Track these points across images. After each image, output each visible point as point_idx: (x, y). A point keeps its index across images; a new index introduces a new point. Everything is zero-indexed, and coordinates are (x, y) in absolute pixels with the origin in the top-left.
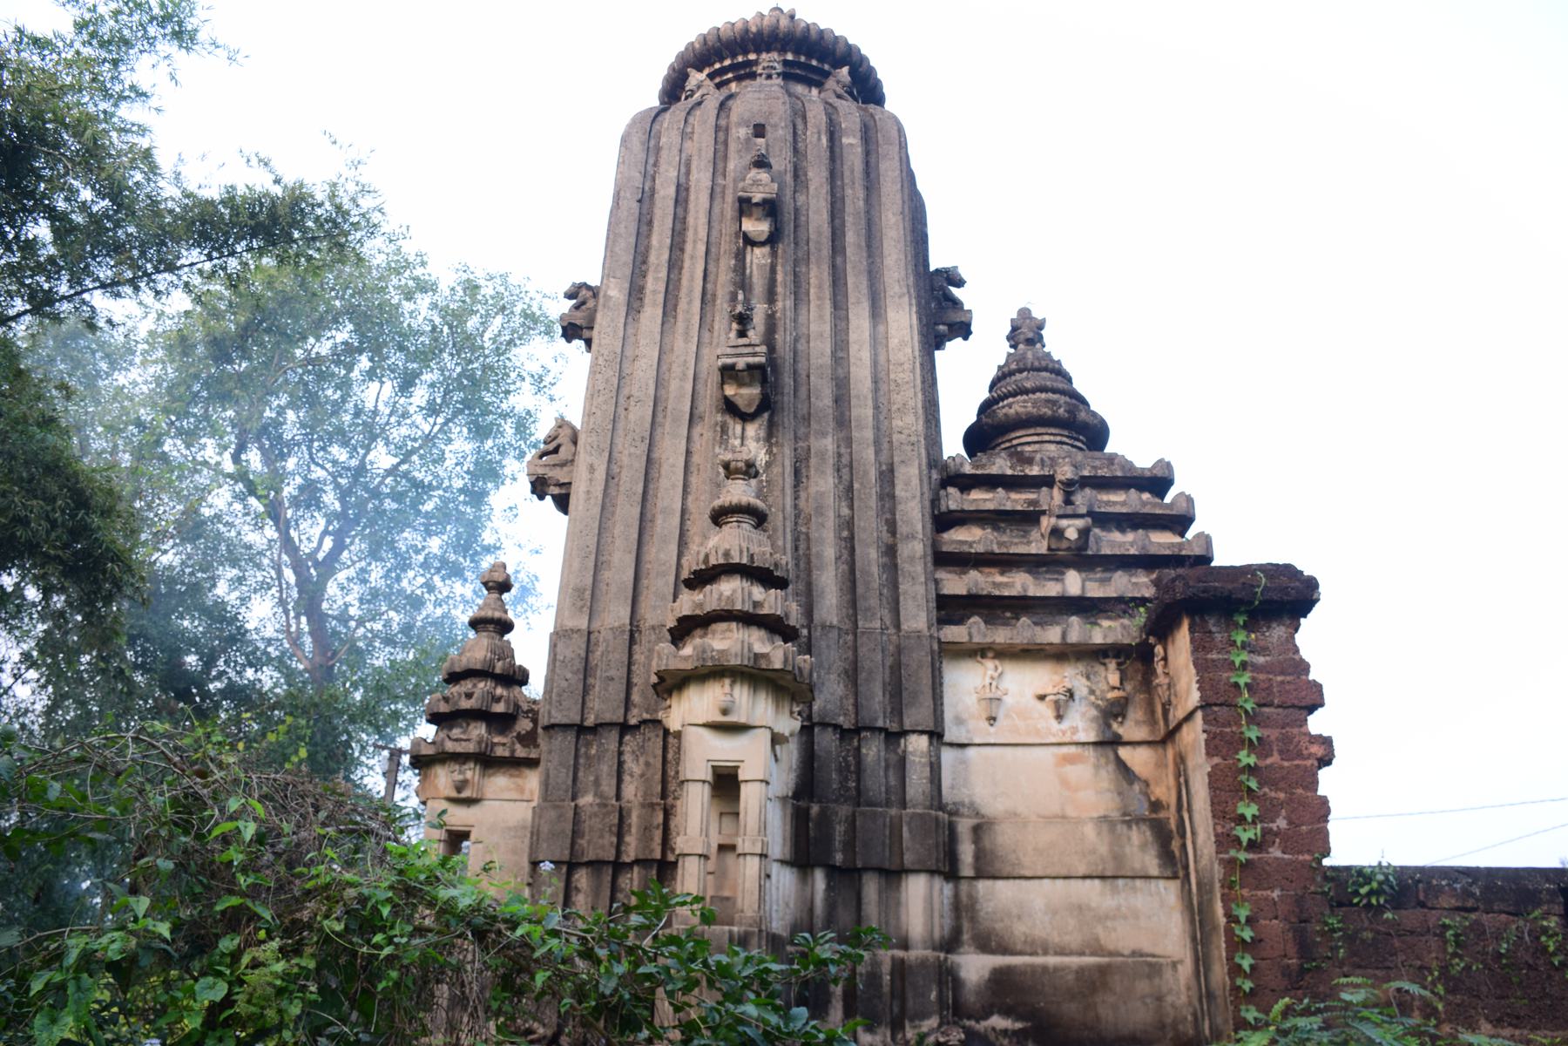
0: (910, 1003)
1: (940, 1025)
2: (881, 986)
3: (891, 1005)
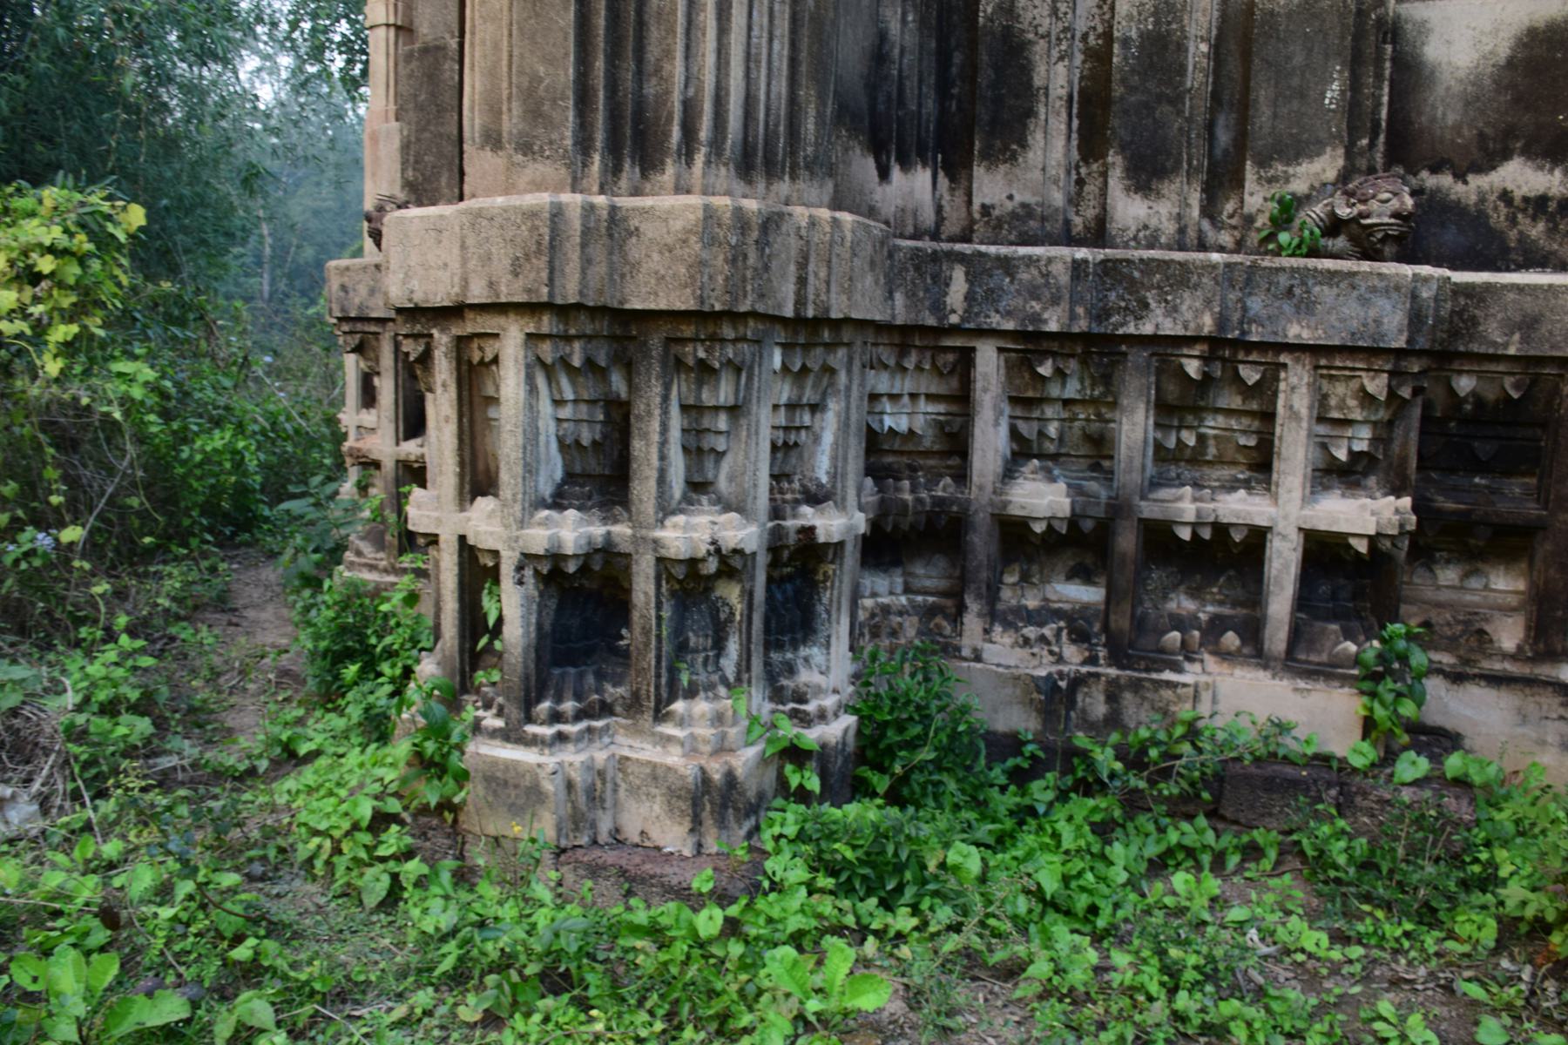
0: (1263, 117)
1: (1344, 177)
2: (1182, 70)
3: (1210, 127)
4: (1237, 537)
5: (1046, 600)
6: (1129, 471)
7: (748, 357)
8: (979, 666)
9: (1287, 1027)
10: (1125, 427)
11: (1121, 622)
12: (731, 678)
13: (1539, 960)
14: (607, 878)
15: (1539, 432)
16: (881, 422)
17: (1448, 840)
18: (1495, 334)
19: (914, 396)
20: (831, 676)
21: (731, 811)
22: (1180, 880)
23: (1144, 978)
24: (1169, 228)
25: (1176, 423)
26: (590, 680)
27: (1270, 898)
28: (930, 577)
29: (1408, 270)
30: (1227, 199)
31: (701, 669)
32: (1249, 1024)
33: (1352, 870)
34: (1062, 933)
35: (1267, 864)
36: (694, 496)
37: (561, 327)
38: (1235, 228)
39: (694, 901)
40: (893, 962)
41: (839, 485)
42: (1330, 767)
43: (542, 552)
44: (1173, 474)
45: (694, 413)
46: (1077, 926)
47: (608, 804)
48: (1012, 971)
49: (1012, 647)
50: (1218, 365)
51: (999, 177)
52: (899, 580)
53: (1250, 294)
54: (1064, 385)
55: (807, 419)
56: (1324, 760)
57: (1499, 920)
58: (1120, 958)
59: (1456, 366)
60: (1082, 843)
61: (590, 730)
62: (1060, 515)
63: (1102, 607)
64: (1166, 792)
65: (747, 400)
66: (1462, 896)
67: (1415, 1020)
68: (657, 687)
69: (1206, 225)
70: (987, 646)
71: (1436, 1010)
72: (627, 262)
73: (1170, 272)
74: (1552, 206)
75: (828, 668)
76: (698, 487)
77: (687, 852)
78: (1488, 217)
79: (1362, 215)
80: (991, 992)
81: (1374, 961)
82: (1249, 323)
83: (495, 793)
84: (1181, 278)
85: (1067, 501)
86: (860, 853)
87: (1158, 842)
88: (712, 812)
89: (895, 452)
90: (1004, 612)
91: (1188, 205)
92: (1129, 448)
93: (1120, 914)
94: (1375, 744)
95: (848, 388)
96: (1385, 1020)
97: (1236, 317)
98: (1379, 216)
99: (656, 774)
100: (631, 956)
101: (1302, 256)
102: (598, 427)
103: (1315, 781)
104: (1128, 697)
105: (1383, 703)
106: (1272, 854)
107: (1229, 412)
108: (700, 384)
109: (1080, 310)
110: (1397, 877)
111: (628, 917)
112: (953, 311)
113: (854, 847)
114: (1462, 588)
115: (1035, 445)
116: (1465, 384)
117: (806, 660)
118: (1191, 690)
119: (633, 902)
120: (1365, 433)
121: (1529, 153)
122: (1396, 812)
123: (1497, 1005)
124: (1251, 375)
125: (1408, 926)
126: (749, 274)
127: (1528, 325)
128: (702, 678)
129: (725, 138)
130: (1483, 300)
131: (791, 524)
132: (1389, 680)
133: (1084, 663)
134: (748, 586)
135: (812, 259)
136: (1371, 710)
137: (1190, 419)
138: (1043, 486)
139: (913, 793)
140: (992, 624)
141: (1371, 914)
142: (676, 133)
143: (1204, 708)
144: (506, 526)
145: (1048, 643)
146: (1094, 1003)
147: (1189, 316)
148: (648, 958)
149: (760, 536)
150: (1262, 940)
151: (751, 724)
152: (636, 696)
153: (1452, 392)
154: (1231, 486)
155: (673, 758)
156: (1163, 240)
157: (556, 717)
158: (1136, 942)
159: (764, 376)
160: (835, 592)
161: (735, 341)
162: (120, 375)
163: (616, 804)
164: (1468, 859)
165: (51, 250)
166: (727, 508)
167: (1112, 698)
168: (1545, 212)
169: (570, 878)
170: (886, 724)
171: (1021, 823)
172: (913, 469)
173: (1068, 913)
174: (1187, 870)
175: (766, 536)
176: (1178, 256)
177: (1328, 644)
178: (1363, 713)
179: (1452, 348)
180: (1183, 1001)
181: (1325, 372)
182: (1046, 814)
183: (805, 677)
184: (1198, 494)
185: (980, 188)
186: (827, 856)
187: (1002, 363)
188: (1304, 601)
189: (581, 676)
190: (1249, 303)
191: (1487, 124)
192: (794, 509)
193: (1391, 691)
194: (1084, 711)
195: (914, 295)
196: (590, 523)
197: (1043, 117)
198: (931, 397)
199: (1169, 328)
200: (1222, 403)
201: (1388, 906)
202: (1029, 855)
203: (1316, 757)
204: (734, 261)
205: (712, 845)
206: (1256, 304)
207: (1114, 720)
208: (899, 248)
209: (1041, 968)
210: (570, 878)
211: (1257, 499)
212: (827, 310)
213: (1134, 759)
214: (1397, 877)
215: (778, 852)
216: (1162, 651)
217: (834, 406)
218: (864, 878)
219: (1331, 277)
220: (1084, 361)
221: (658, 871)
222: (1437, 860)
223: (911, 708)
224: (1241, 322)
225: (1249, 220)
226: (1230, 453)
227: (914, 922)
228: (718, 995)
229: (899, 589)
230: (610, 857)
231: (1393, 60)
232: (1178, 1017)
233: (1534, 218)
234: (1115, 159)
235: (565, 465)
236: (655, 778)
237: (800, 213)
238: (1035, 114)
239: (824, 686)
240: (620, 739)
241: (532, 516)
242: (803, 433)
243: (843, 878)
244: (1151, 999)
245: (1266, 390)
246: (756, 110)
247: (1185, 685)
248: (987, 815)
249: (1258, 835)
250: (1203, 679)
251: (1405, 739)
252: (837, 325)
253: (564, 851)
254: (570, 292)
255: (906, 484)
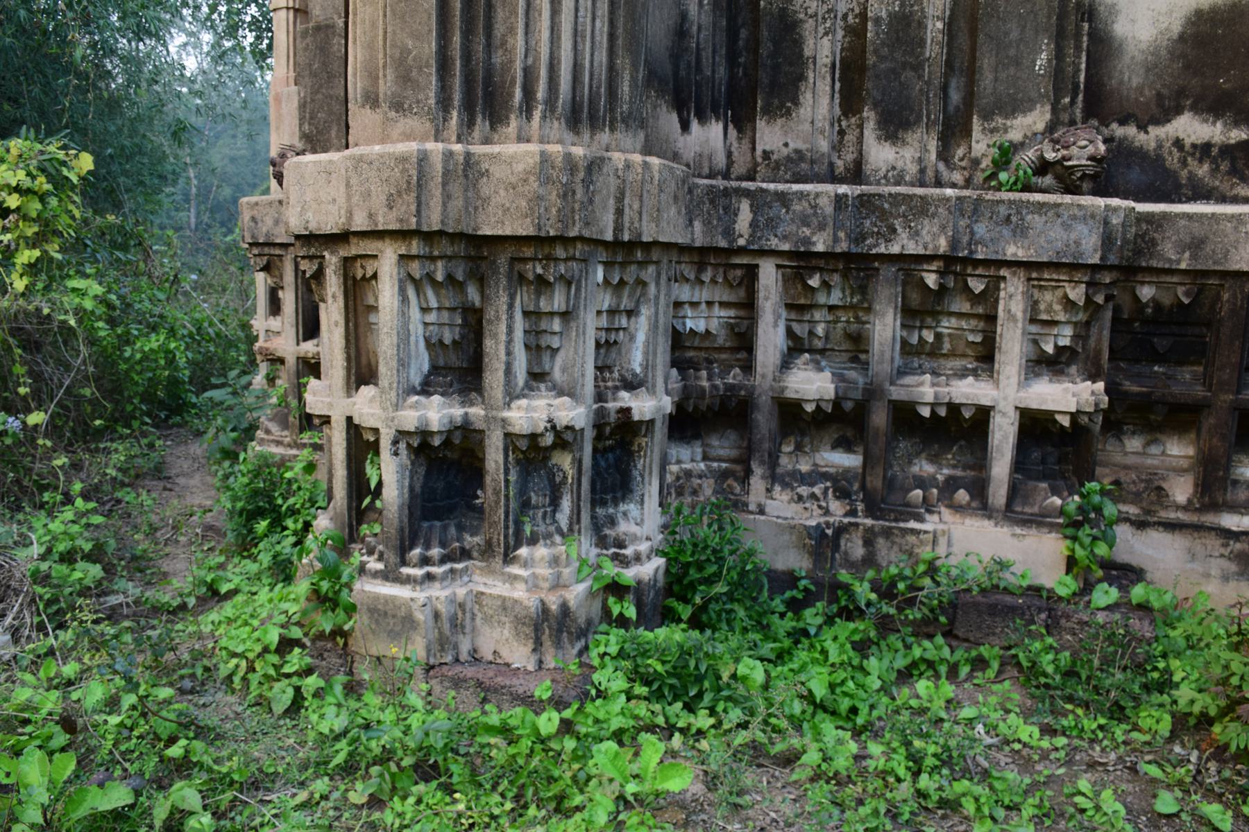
0: (986, 80)
1: (1051, 128)
2: (922, 42)
3: (945, 88)
4: (967, 414)
5: (815, 465)
6: (881, 362)
7: (577, 272)
8: (763, 518)
9: (1007, 802)
10: (878, 328)
11: (875, 481)
12: (565, 530)
13: (1204, 746)
14: (467, 689)
15: (1205, 330)
16: (684, 324)
17: (1133, 652)
18: (1170, 252)
19: (710, 304)
20: (645, 527)
21: (565, 634)
22: (923, 686)
23: (895, 764)
24: (913, 169)
25: (918, 324)
26: (452, 531)
27: (993, 700)
28: (723, 448)
29: (1101, 202)
30: (959, 146)
31: (541, 522)
32: (977, 800)
33: (1058, 677)
34: (828, 728)
35: (991, 673)
36: (535, 384)
37: (427, 249)
38: (964, 169)
39: (537, 707)
40: (695, 753)
41: (650, 375)
42: (1041, 596)
43: (413, 429)
44: (916, 365)
45: (533, 318)
46: (841, 723)
47: (467, 630)
48: (789, 760)
49: (789, 503)
50: (952, 277)
51: (777, 129)
52: (699, 450)
53: (977, 221)
54: (829, 294)
55: (624, 322)
56: (1036, 590)
57: (1173, 715)
58: (875, 749)
59: (1139, 278)
60: (845, 658)
61: (452, 571)
62: (827, 397)
63: (860, 471)
64: (911, 617)
65: (576, 307)
66: (1145, 697)
67: (1107, 794)
68: (506, 536)
69: (941, 166)
70: (769, 502)
71: (1124, 787)
72: (479, 197)
73: (913, 203)
74: (1215, 151)
75: (642, 520)
76: (537, 376)
77: (531, 668)
78: (1164, 160)
79: (1064, 158)
80: (773, 776)
81: (1075, 749)
82: (976, 244)
83: (377, 622)
84: (922, 208)
85: (833, 386)
86: (668, 667)
87: (905, 656)
88: (550, 636)
89: (695, 348)
90: (782, 475)
91: (927, 151)
92: (881, 344)
93: (875, 713)
94: (1076, 578)
95: (657, 298)
96: (1084, 795)
97: (965, 239)
98: (1078, 159)
99: (505, 605)
100: (486, 751)
101: (1017, 191)
102: (458, 329)
103: (1029, 607)
104: (881, 541)
105: (1082, 545)
106: (995, 665)
107: (960, 315)
108: (538, 294)
109: (842, 235)
110: (1093, 682)
111: (484, 719)
112: (741, 236)
113: (664, 663)
114: (1144, 453)
115: (806, 342)
116: (1146, 293)
117: (625, 514)
118: (931, 536)
119: (488, 707)
120: (1068, 331)
121: (1196, 109)
122: (1092, 631)
123: (1171, 782)
124: (977, 286)
125: (1102, 721)
126: (577, 206)
127: (1196, 245)
128: (542, 528)
129: (557, 98)
130: (1161, 226)
131: (612, 406)
132: (1087, 526)
133: (846, 515)
134: (577, 456)
135: (627, 194)
136: (1073, 550)
137: (929, 320)
138: (812, 375)
139: (710, 619)
140: (773, 485)
141: (1073, 712)
142: (518, 94)
143: (941, 550)
144: (384, 409)
145: (818, 499)
146: (855, 784)
147: (928, 238)
148: (500, 752)
149: (587, 416)
150: (987, 733)
151: (581, 565)
152: (489, 543)
153: (1137, 299)
154: (962, 374)
155: (519, 593)
156: (907, 178)
157: (425, 561)
158: (888, 735)
159: (589, 288)
160: (648, 460)
161: (566, 260)
162: (74, 290)
163: (474, 629)
164: (1149, 668)
165: (17, 189)
166: (561, 393)
167: (868, 542)
168: (1209, 156)
169: (437, 689)
170: (688, 564)
171: (797, 642)
172: (710, 361)
173: (834, 713)
174: (928, 679)
175: (592, 415)
176: (919, 191)
177: (1039, 499)
178: (1067, 553)
179: (1136, 264)
180: (924, 781)
181: (1036, 283)
182: (816, 635)
183: (624, 527)
184: (936, 380)
185: (762, 138)
186: (642, 670)
187: (780, 277)
188: (1019, 465)
189: (445, 528)
190: (975, 228)
191: (1164, 86)
192: (614, 394)
193: (1089, 535)
194: (846, 553)
195: (709, 223)
196: (451, 406)
197: (811, 81)
198: (722, 304)
199: (912, 248)
200: (955, 308)
201: (1086, 705)
202: (803, 668)
203: (1030, 588)
204: (565, 195)
205: (551, 662)
206: (981, 229)
207: (870, 560)
208: (697, 186)
209: (812, 757)
210: (437, 689)
211: (983, 384)
212: (640, 235)
213: (886, 591)
214: (1093, 682)
215: (603, 666)
216: (908, 505)
217: (646, 312)
218: (672, 687)
219: (1041, 206)
220: (845, 275)
221: (508, 683)
222: (1125, 669)
223: (709, 552)
224: (970, 244)
225: (976, 162)
226: (961, 348)
227: (712, 721)
228: (556, 780)
229: (699, 457)
230: (469, 672)
231: (1089, 35)
232: (921, 794)
233: (1201, 161)
234: (869, 114)
235: (431, 359)
236: (505, 609)
237: (618, 157)
238: (806, 79)
239: (639, 534)
240: (476, 578)
241: (405, 400)
242: (621, 333)
243: (655, 687)
244: (899, 780)
245: (989, 297)
246: (582, 74)
247: (926, 532)
248: (769, 636)
249: (984, 651)
250: (940, 527)
251: (1100, 573)
252: (648, 246)
253: (433, 667)
254: (434, 221)
255: (704, 373)
